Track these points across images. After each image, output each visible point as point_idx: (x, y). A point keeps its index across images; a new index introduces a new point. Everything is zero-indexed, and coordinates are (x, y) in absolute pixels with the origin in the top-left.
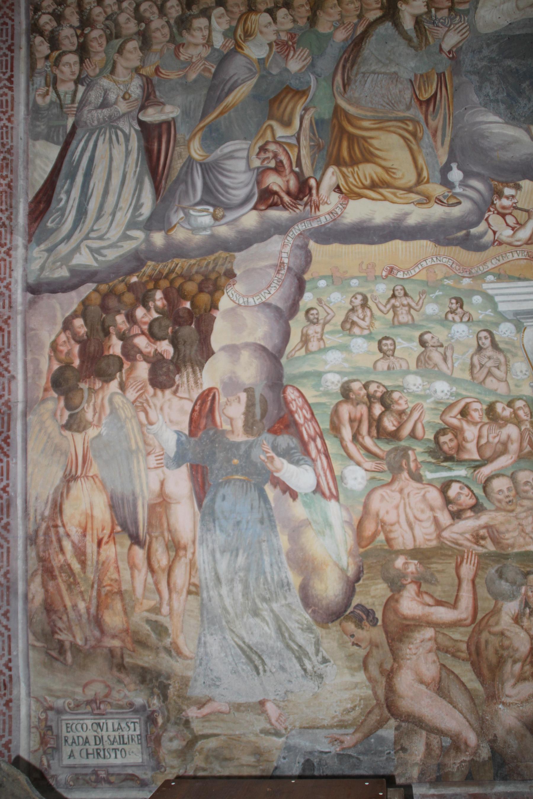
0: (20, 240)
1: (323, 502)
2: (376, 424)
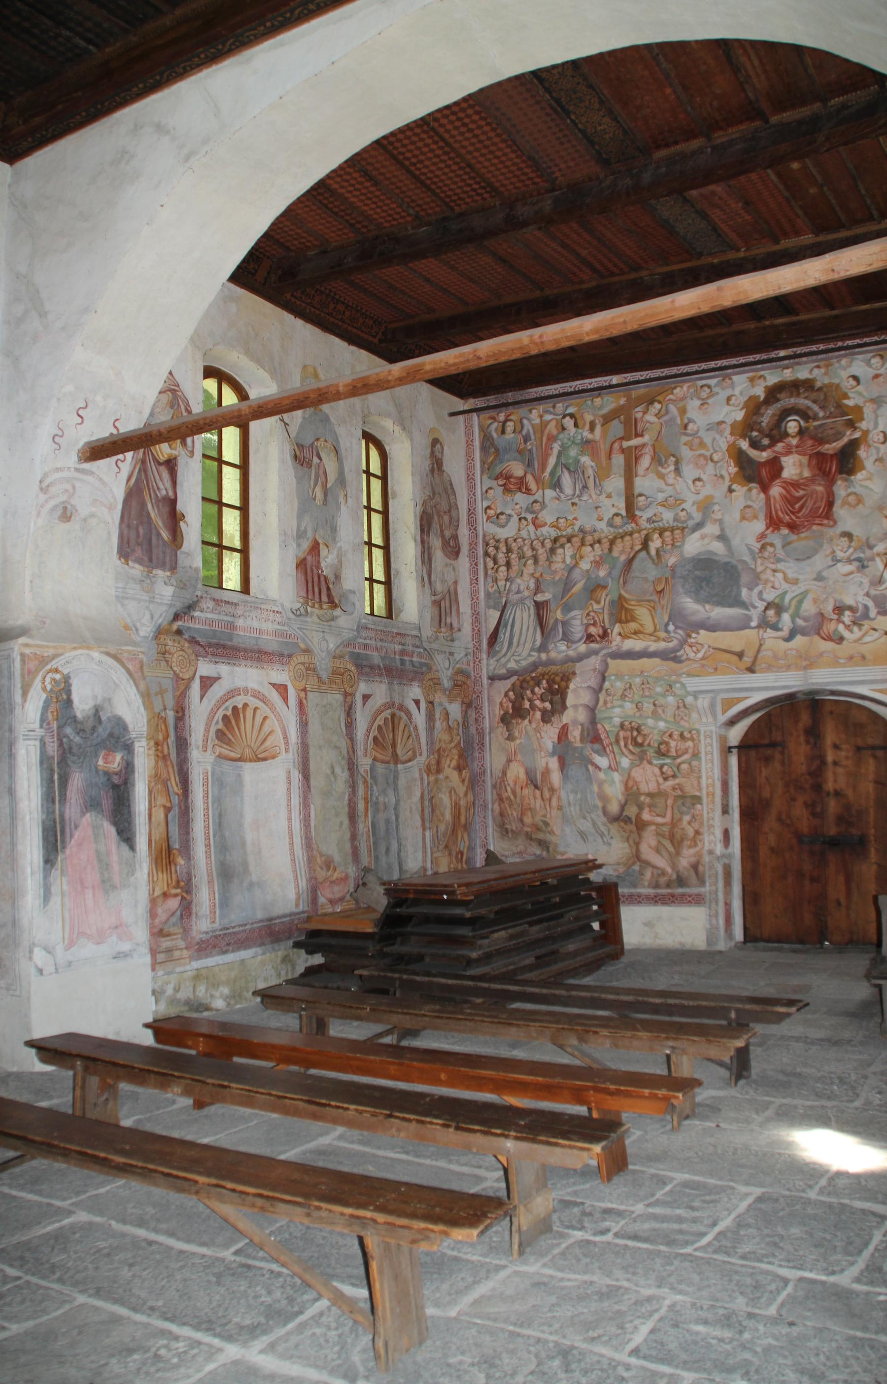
0: (484, 656)
2: (634, 739)
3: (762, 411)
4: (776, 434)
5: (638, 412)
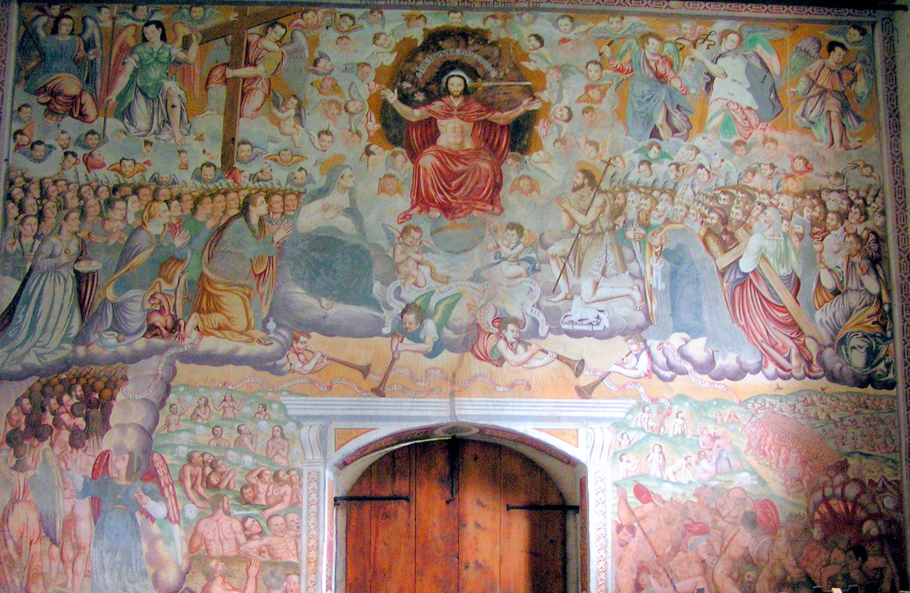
1: (170, 525)
3: (420, 57)
4: (434, 89)
5: (253, 34)
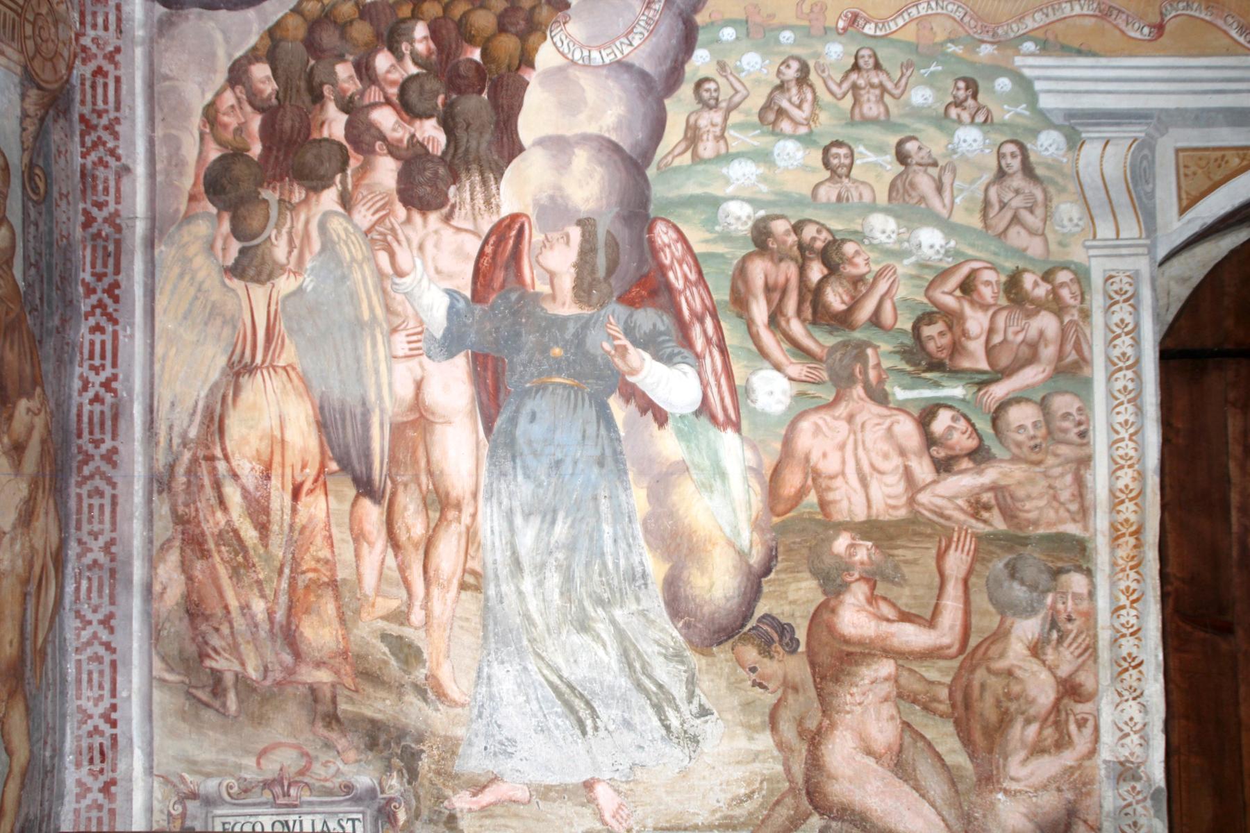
1: (713, 432)
2: (813, 298)
